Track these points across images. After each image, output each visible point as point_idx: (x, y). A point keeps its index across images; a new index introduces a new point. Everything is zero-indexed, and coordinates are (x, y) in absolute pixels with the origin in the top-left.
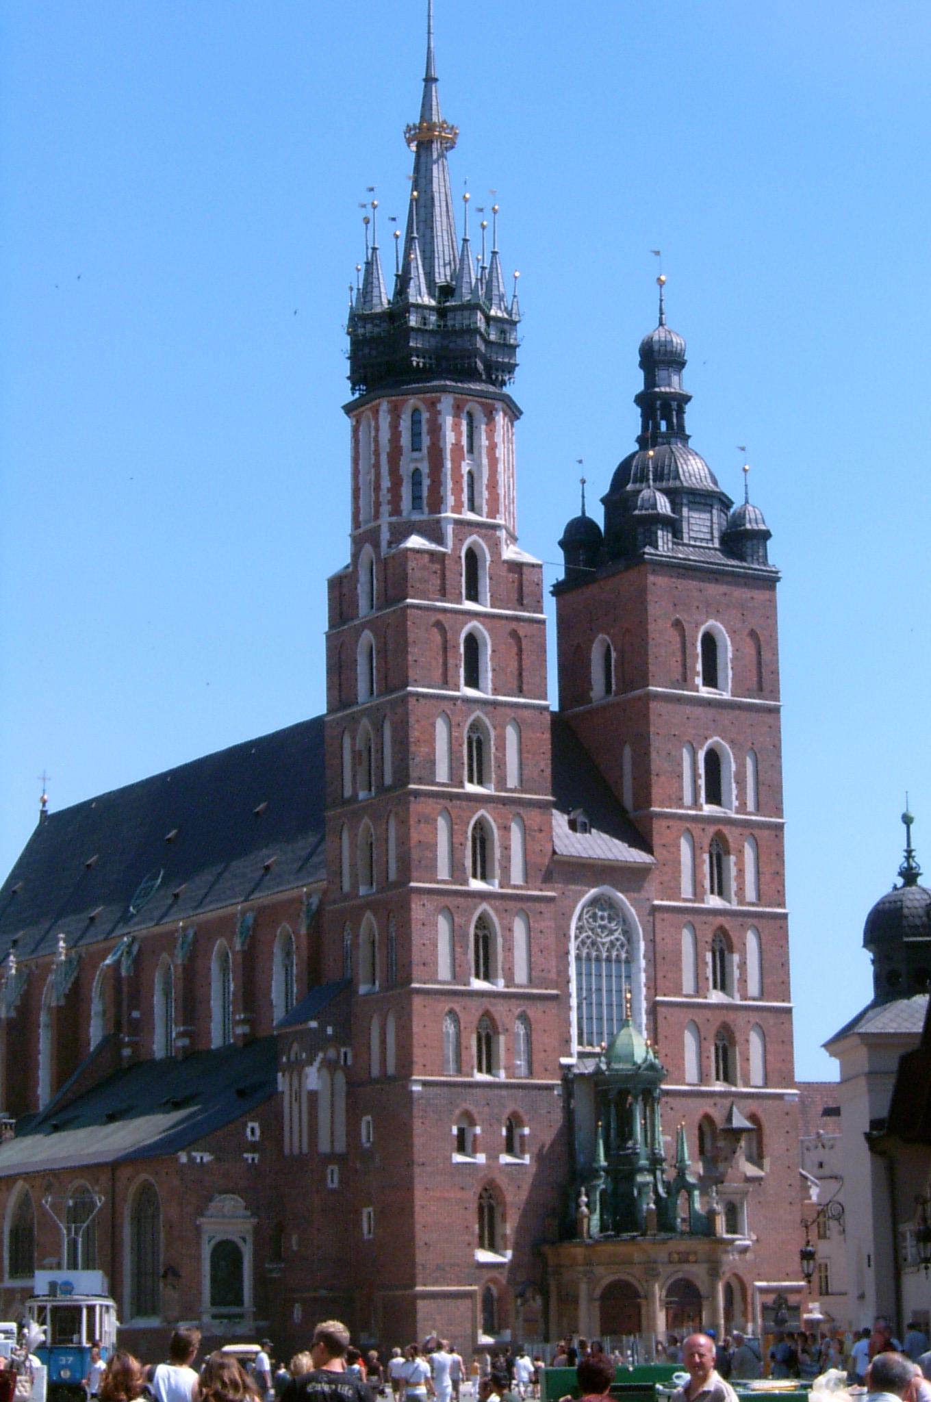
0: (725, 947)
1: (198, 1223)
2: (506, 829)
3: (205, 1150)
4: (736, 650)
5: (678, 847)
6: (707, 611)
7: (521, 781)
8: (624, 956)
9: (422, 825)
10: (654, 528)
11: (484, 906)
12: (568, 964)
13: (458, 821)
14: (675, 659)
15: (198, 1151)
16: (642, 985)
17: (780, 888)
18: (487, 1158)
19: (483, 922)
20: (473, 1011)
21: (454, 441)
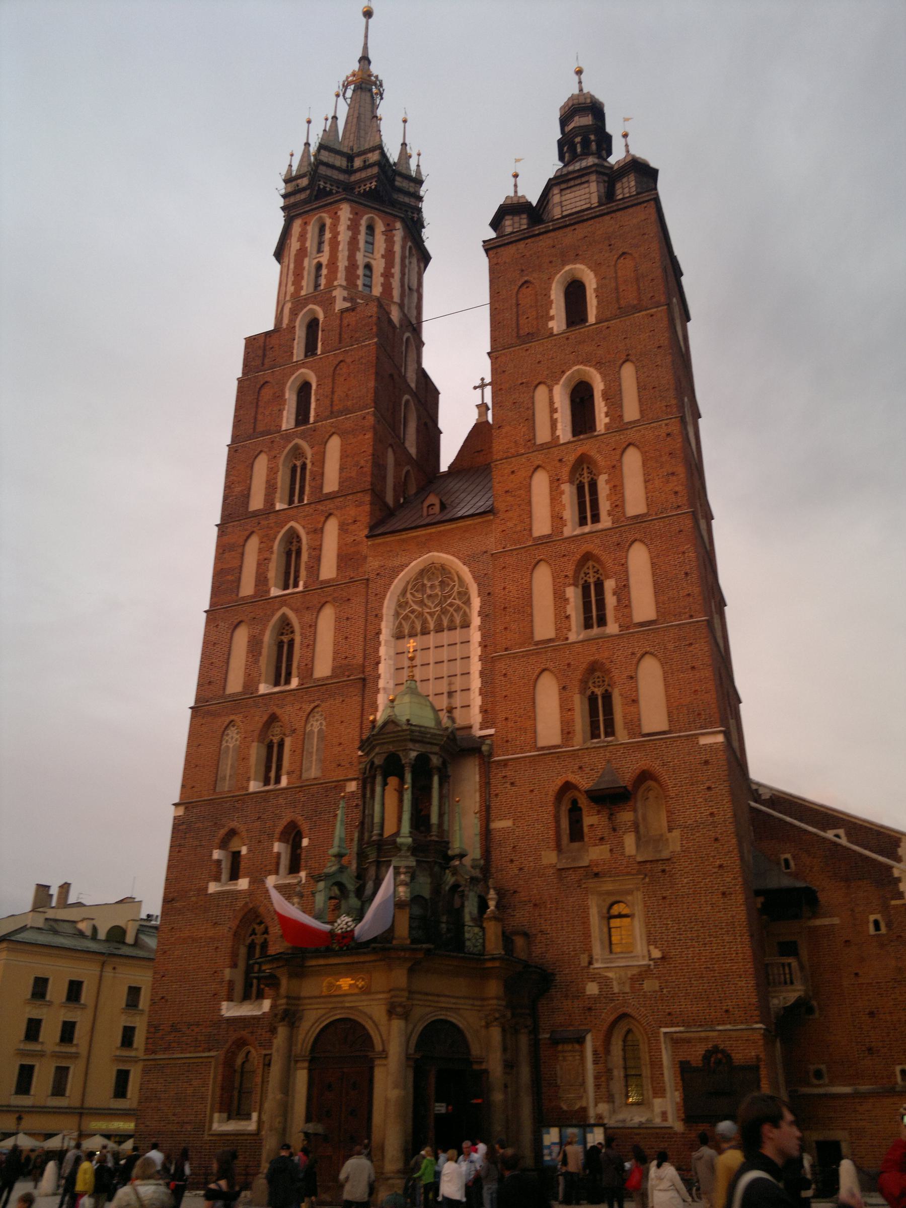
0: (602, 578)
2: (317, 532)
4: (601, 278)
7: (340, 482)
8: (458, 619)
9: (226, 555)
10: (503, 223)
11: (285, 610)
12: (379, 643)
13: (263, 540)
14: (525, 317)
16: (477, 645)
17: (677, 489)
19: (285, 625)
20: (257, 718)
21: (298, 248)
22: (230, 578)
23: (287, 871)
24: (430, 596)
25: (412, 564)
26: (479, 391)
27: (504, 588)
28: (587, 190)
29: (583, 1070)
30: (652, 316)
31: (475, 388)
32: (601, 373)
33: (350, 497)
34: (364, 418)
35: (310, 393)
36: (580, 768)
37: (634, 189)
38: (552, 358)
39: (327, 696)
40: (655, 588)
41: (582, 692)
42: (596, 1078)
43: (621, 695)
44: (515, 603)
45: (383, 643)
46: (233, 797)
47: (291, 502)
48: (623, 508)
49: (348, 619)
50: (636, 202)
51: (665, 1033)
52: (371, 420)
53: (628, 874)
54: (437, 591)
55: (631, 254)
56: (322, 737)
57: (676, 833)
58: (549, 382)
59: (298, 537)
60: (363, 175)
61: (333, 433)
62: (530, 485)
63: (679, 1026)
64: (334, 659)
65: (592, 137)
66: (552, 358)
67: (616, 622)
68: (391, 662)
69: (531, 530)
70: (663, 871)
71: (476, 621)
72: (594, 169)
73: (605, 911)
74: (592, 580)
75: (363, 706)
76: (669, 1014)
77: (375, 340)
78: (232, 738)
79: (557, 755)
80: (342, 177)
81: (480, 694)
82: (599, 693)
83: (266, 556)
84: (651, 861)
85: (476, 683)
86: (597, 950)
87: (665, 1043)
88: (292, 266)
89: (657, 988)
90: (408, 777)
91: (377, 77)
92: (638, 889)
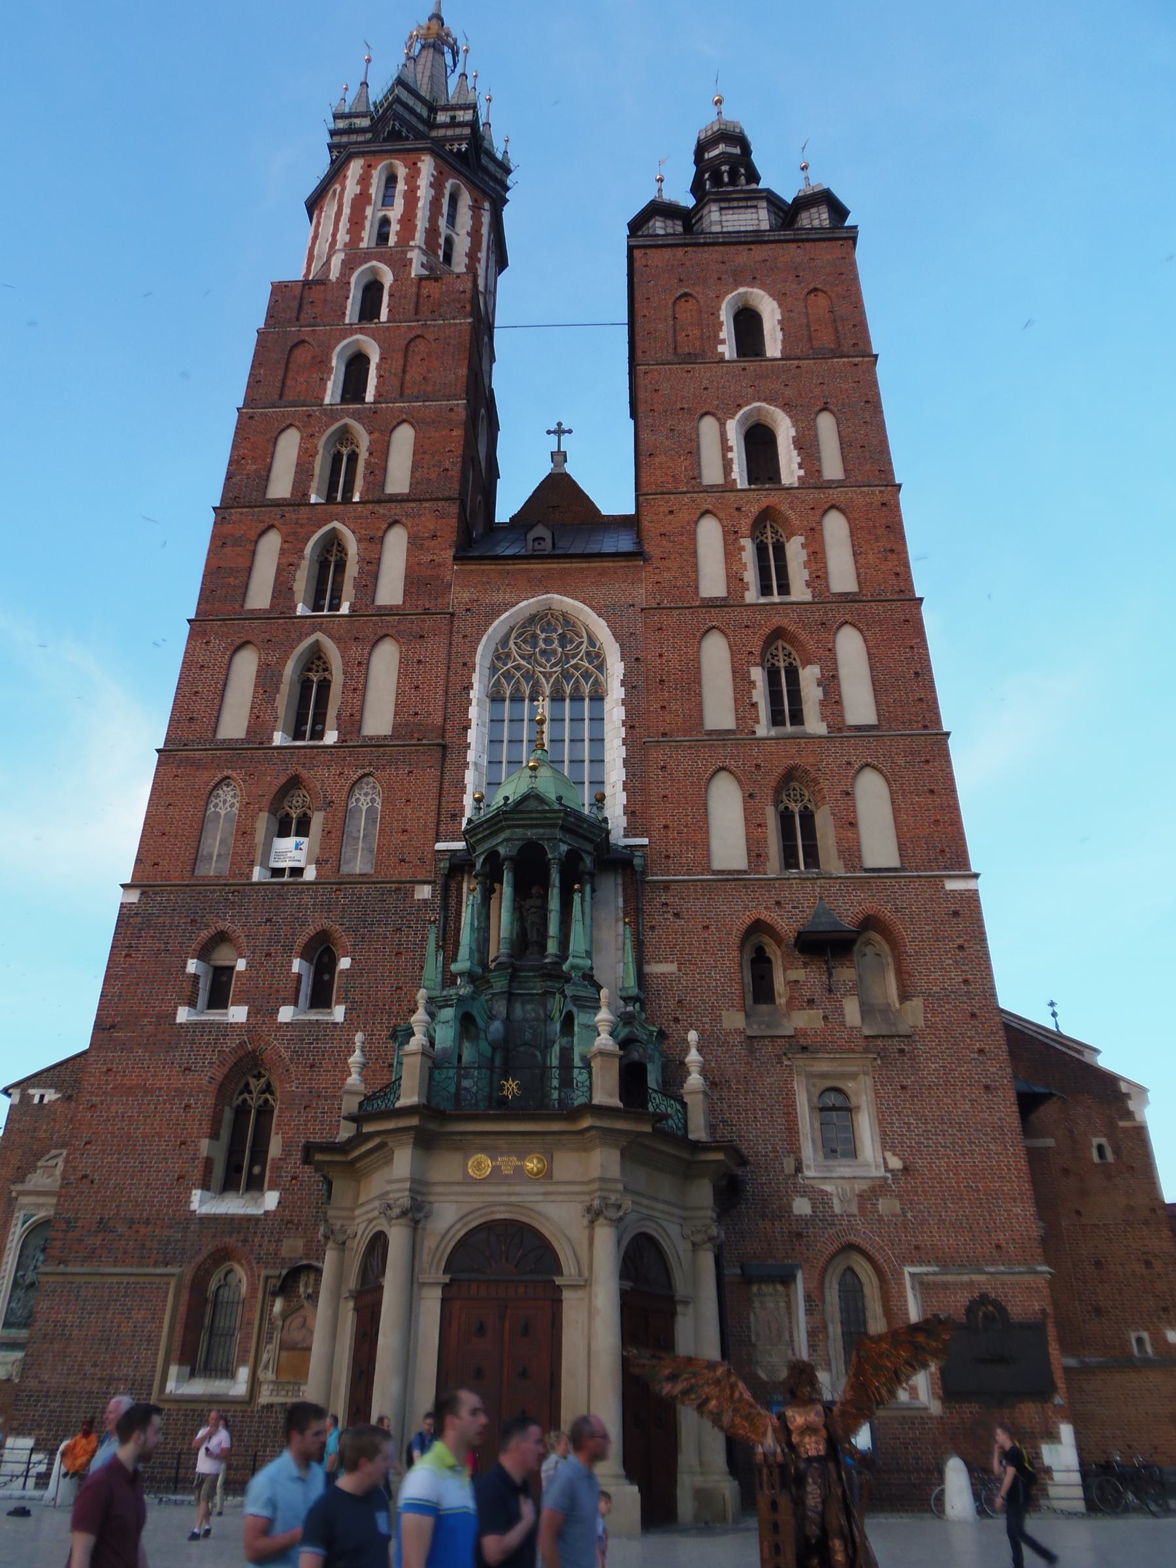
0: (798, 663)
1: (14, 1194)
2: (374, 542)
3: (50, 1087)
5: (693, 536)
6: (735, 280)
7: (411, 484)
8: (586, 689)
9: (228, 550)
10: (651, 223)
11: (319, 635)
12: (469, 702)
14: (684, 334)
15: (39, 1086)
17: (898, 570)
18: (249, 1013)
19: (316, 657)
22: (231, 580)
23: (308, 1005)
24: (543, 652)
25: (522, 604)
26: (554, 437)
27: (660, 655)
28: (755, 216)
29: (790, 1322)
30: (856, 365)
31: (549, 432)
32: (790, 417)
33: (427, 505)
34: (451, 410)
35: (367, 370)
36: (778, 903)
37: (828, 222)
38: (724, 387)
39: (384, 762)
40: (874, 684)
41: (777, 802)
42: (812, 1334)
43: (833, 814)
44: (677, 676)
45: (474, 702)
46: (225, 885)
47: (330, 499)
48: (826, 579)
49: (419, 662)
50: (830, 236)
51: (912, 1275)
52: (461, 414)
53: (853, 1051)
54: (556, 644)
55: (825, 292)
56: (371, 819)
57: (917, 1003)
58: (720, 414)
59: (339, 544)
60: (450, 132)
61: (404, 421)
62: (695, 533)
63: (932, 1265)
64: (396, 714)
65: (742, 171)
66: (724, 387)
67: (823, 721)
68: (486, 731)
69: (697, 587)
70: (902, 1051)
71: (615, 692)
72: (764, 194)
73: (815, 1100)
74: (782, 665)
75: (441, 784)
76: (917, 1248)
77: (470, 320)
78: (225, 802)
79: (742, 883)
80: (421, 127)
81: (624, 790)
82: (797, 810)
83: (291, 560)
84: (883, 1037)
85: (615, 774)
86: (808, 1151)
87: (913, 1288)
88: (347, 211)
89: (898, 1211)
90: (555, 877)
91: (455, 41)
92: (865, 1073)
